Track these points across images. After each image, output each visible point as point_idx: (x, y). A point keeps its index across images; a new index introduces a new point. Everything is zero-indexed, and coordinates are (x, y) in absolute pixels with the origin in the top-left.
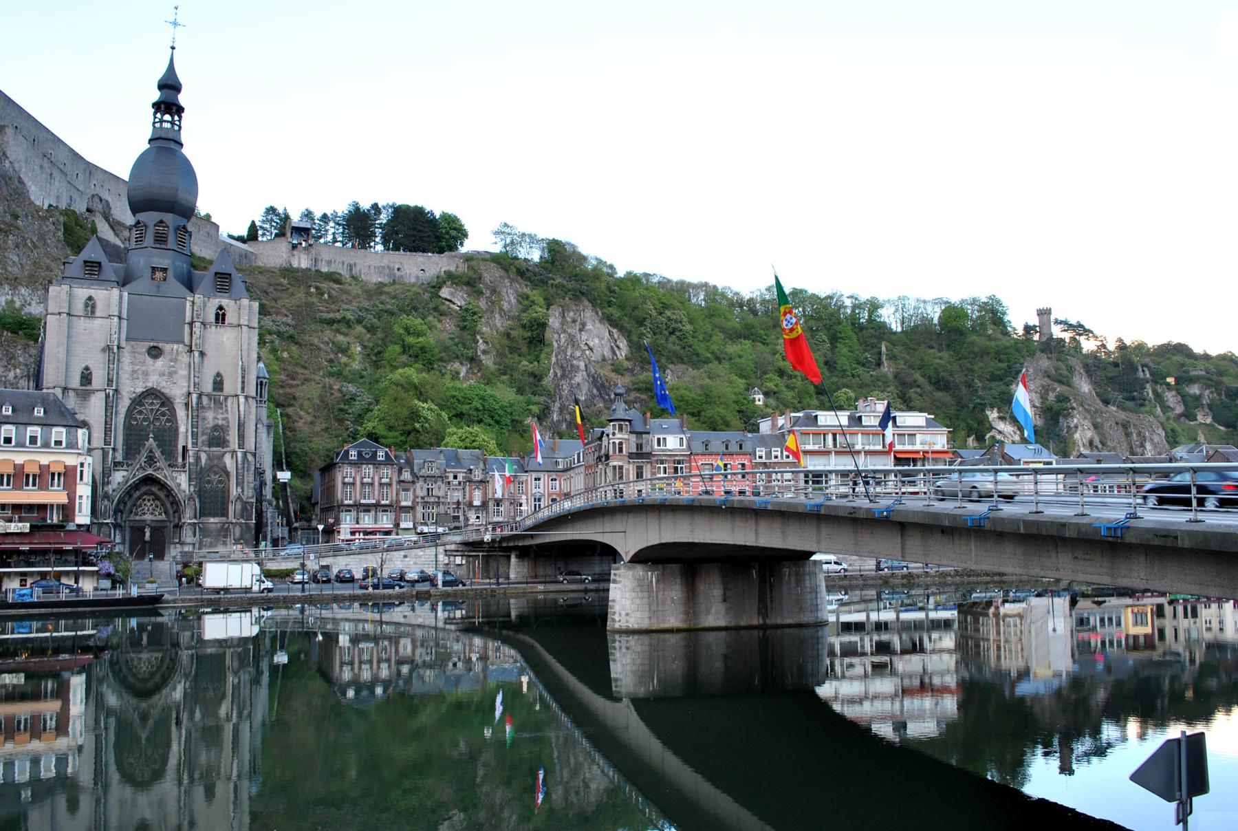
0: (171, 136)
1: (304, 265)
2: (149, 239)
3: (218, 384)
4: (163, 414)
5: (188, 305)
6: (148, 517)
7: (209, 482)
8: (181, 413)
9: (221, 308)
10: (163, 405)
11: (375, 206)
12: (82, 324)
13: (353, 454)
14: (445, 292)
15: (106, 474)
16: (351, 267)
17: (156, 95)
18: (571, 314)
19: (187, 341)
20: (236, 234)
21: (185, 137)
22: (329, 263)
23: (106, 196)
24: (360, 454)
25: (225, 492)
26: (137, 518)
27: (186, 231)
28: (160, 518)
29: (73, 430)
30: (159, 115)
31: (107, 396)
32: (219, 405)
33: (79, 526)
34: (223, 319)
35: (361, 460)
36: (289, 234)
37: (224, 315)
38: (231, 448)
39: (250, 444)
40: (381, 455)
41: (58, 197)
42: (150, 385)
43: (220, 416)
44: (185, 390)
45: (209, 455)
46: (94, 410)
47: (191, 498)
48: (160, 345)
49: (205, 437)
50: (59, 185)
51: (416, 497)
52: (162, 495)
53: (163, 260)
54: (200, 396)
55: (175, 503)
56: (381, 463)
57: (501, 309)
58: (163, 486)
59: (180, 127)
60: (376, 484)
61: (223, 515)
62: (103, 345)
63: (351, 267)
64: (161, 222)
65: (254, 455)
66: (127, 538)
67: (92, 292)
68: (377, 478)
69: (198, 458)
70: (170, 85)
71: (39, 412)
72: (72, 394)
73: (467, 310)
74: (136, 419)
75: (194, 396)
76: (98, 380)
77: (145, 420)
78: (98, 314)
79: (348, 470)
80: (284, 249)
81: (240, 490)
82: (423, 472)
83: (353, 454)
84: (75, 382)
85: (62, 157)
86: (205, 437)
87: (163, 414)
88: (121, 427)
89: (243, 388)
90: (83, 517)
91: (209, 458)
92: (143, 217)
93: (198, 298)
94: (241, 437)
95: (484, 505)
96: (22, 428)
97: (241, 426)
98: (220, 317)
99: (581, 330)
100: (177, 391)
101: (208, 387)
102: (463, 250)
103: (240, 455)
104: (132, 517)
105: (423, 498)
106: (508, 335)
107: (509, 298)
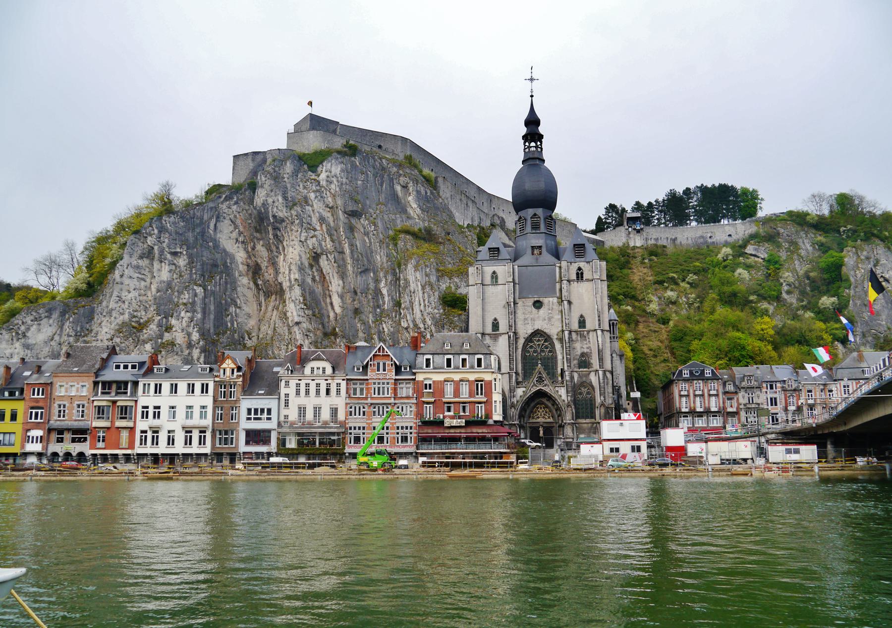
0: (536, 156)
1: (638, 244)
2: (529, 228)
3: (582, 323)
5: (557, 269)
6: (541, 420)
7: (581, 394)
9: (580, 269)
10: (546, 341)
11: (687, 191)
12: (490, 290)
13: (686, 374)
14: (750, 249)
15: (512, 390)
16: (674, 240)
17: (524, 130)
18: (865, 253)
20: (588, 230)
21: (545, 155)
22: (657, 240)
23: (501, 214)
24: (691, 373)
25: (593, 400)
26: (534, 421)
27: (552, 219)
28: (548, 420)
29: (488, 356)
30: (527, 144)
31: (509, 337)
32: (583, 337)
33: (495, 422)
34: (582, 277)
35: (692, 378)
36: (625, 223)
37: (582, 274)
38: (594, 369)
39: (608, 366)
40: (708, 373)
41: (472, 219)
42: (536, 328)
43: (585, 346)
44: (560, 329)
46: (501, 346)
47: (568, 406)
48: (541, 299)
49: (576, 362)
50: (472, 211)
51: (739, 404)
52: (550, 405)
53: (538, 240)
54: (570, 332)
55: (558, 409)
56: (708, 379)
57: (799, 255)
58: (549, 397)
59: (541, 149)
60: (706, 395)
61: (592, 418)
62: (504, 302)
63: (674, 240)
64: (535, 215)
65: (612, 373)
66: (528, 435)
67: (495, 268)
68: (706, 391)
69: (572, 377)
70: (532, 122)
71: (467, 347)
72: (487, 337)
73: (769, 261)
74: (529, 352)
75: (566, 333)
76: (503, 327)
77: (535, 352)
78: (500, 282)
79: (683, 385)
80: (624, 235)
81: (602, 398)
82: (744, 384)
83: (686, 374)
84: (489, 330)
85: (472, 193)
88: (519, 358)
89: (599, 325)
90: (497, 416)
91: (580, 376)
92: (521, 213)
93: (564, 264)
94: (601, 360)
95: (799, 409)
96: (457, 356)
97: (600, 352)
98: (580, 276)
99: (875, 266)
100: (553, 330)
101: (575, 326)
102: (761, 214)
103: (601, 373)
104: (531, 421)
105: (745, 405)
106: (808, 278)
107: (807, 244)
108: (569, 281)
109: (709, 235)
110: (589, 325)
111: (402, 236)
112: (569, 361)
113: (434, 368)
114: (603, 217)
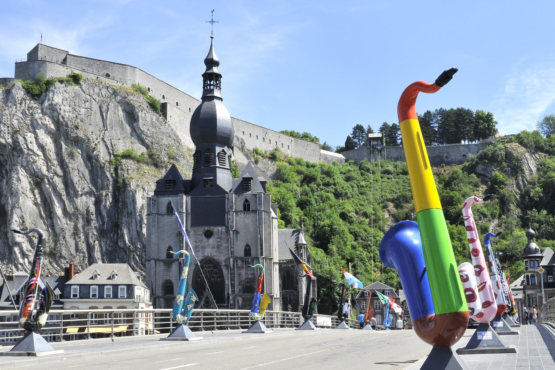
3: (248, 251)
4: (216, 273)
8: (225, 272)
9: (246, 201)
19: (226, 224)
37: (249, 205)
42: (206, 254)
45: (243, 299)
49: (240, 287)
54: (236, 259)
72: (162, 264)
75: (231, 260)
86: (240, 287)
87: (216, 273)
100: (221, 258)
101: (242, 253)
108: (236, 212)
109: (445, 155)
110: (253, 253)
111: (124, 161)
112: (233, 286)
113: (81, 298)
114: (351, 136)
